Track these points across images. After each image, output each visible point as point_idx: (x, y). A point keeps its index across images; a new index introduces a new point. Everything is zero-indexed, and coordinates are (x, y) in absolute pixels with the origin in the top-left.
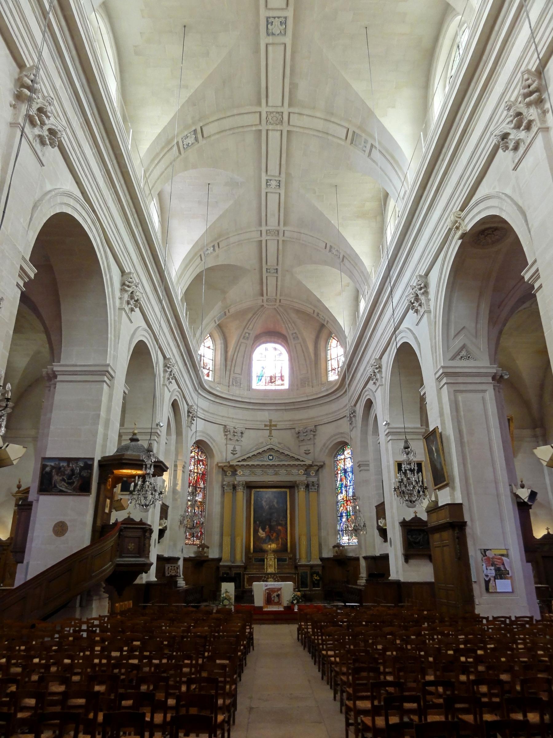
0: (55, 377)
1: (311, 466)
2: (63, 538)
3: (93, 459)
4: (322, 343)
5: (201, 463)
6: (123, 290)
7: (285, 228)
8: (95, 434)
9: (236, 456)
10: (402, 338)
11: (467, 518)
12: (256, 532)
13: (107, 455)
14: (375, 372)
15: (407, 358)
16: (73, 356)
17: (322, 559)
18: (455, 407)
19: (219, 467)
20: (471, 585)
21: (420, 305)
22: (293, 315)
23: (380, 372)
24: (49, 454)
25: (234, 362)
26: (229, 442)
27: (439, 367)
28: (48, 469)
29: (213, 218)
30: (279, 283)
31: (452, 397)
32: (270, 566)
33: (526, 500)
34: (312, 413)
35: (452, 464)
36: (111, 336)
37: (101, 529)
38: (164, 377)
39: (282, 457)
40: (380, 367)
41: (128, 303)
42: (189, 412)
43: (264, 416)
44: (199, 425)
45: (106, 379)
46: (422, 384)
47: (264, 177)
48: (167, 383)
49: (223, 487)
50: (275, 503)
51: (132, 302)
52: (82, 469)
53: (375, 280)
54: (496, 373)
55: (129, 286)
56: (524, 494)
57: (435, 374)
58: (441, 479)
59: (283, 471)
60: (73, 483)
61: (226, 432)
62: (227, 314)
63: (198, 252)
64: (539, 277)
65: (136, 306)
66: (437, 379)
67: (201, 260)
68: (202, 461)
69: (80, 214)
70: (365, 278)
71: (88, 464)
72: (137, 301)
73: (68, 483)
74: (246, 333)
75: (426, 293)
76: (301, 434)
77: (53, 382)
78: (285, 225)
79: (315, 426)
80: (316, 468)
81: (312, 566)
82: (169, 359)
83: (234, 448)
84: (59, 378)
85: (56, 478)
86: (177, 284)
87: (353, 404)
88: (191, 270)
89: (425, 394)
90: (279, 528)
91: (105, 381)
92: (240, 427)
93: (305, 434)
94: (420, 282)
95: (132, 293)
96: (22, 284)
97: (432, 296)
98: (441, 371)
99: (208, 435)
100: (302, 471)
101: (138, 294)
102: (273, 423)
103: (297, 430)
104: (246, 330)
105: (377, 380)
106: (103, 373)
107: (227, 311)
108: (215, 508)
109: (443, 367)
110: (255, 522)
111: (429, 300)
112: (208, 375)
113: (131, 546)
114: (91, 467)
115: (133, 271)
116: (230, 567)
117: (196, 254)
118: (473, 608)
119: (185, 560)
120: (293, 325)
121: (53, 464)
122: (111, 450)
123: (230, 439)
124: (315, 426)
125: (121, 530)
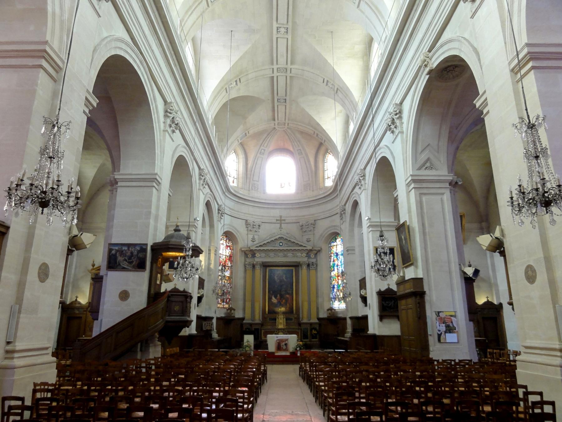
0: (117, 183)
1: (311, 250)
2: (126, 302)
3: (146, 245)
4: (320, 157)
5: (229, 248)
6: (166, 116)
7: (292, 67)
8: (148, 226)
9: (255, 243)
10: (381, 153)
11: (426, 289)
12: (270, 299)
13: (157, 241)
15: (385, 168)
16: (130, 167)
17: (319, 319)
18: (420, 205)
19: (242, 251)
20: (427, 337)
21: (396, 127)
22: (299, 136)
23: (364, 179)
24: (114, 241)
25: (253, 172)
26: (249, 232)
27: (409, 175)
28: (113, 252)
29: (235, 59)
30: (287, 111)
31: (418, 199)
32: (281, 323)
33: (471, 276)
35: (415, 249)
36: (158, 151)
37: (154, 296)
38: (199, 183)
39: (289, 244)
40: (364, 176)
41: (170, 126)
42: (219, 210)
43: (276, 213)
44: (227, 219)
45: (155, 184)
46: (396, 188)
47: (275, 25)
48: (202, 188)
49: (245, 267)
50: (284, 278)
51: (173, 125)
52: (139, 252)
53: (362, 107)
54: (452, 180)
55: (170, 113)
56: (470, 271)
57: (406, 180)
58: (408, 260)
59: (290, 254)
60: (132, 262)
62: (247, 134)
63: (224, 86)
64: (487, 105)
65: (176, 129)
67: (227, 92)
68: (229, 246)
69: (131, 56)
70: (354, 106)
71: (142, 248)
72: (177, 124)
73: (129, 263)
75: (400, 118)
77: (115, 187)
78: (292, 63)
80: (315, 252)
81: (311, 324)
82: (203, 170)
83: (254, 237)
84: (120, 184)
85: (120, 258)
87: (343, 204)
88: (219, 100)
89: (397, 196)
90: (287, 296)
91: (154, 186)
92: (258, 221)
94: (395, 109)
95: (173, 118)
96: (87, 111)
97: (405, 119)
99: (233, 227)
100: (304, 254)
101: (177, 119)
102: (283, 218)
103: (301, 223)
104: (262, 148)
105: (362, 185)
106: (152, 180)
107: (247, 132)
108: (239, 281)
109: (411, 175)
110: (269, 292)
111: (403, 123)
112: (233, 182)
113: (177, 308)
114: (145, 250)
115: (173, 101)
116: (251, 325)
117: (222, 88)
118: (429, 354)
119: (218, 319)
121: (117, 248)
122: (160, 238)
123: (251, 231)
125: (169, 297)
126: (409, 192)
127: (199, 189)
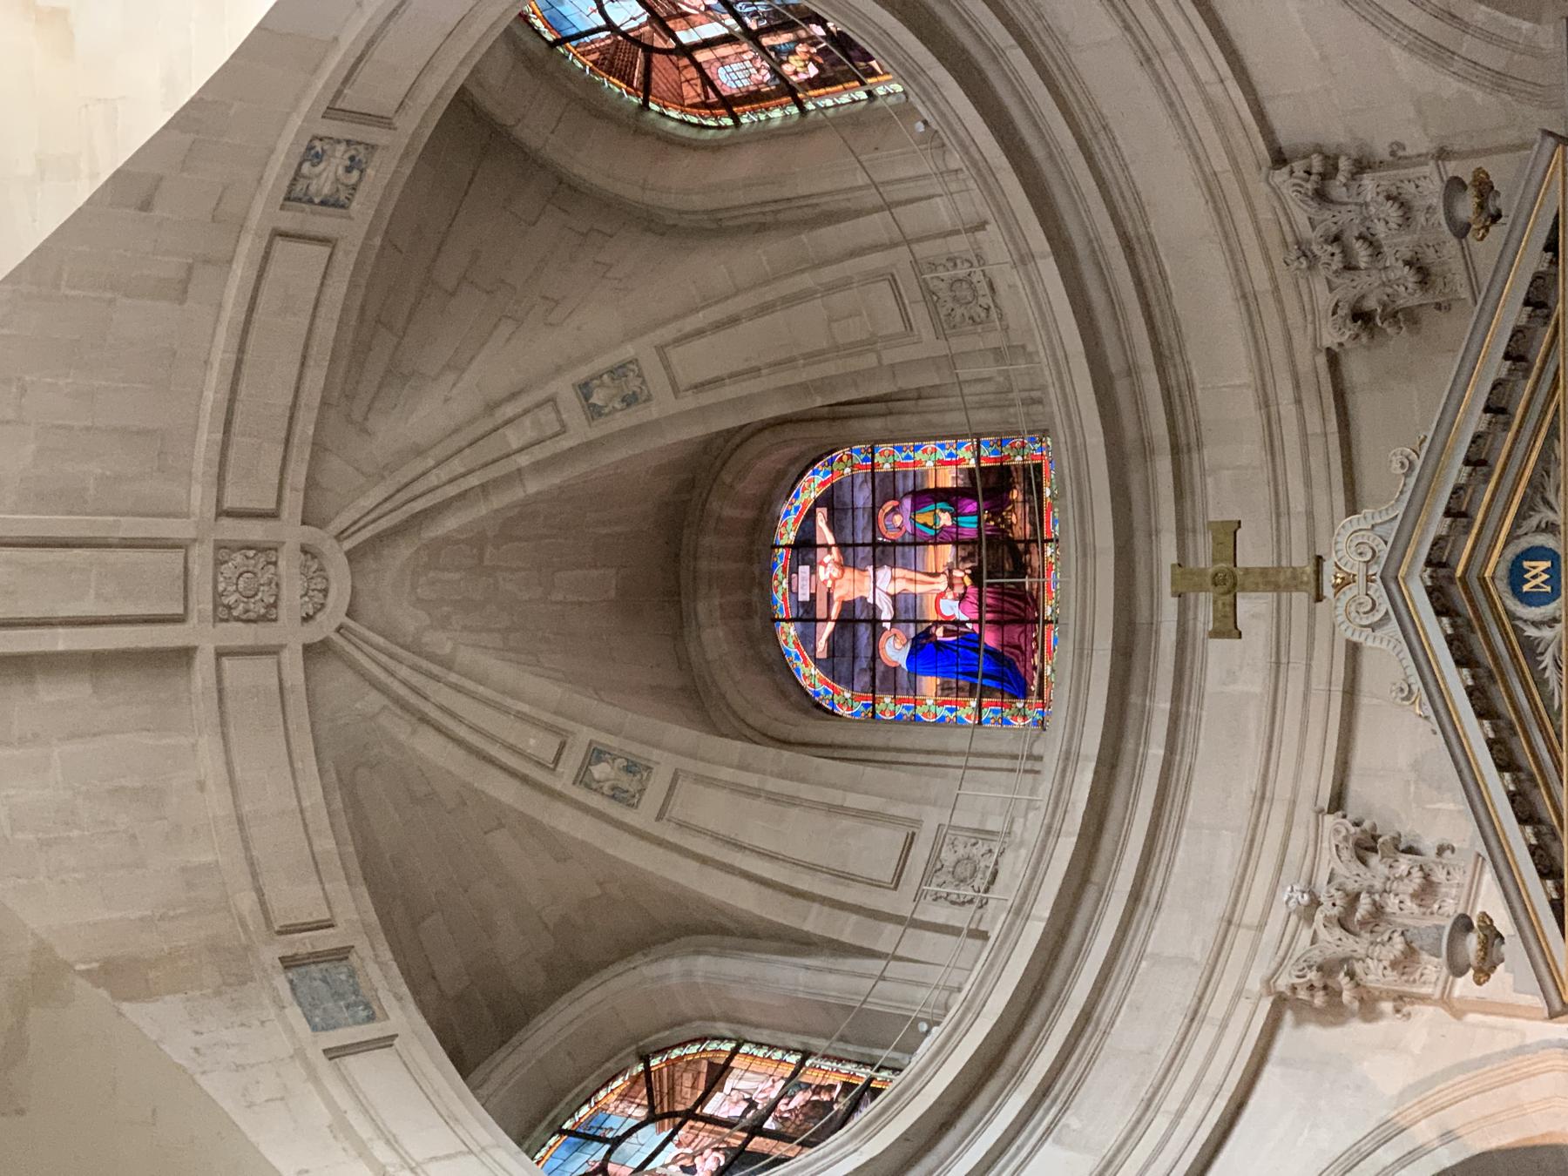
25: (804, 882)
34: (1176, 209)
61: (1333, 993)
74: (583, 778)
76: (1370, 288)
79: (1280, 159)
93: (1362, 254)
104: (563, 781)
120: (509, 410)
124: (1280, 159)
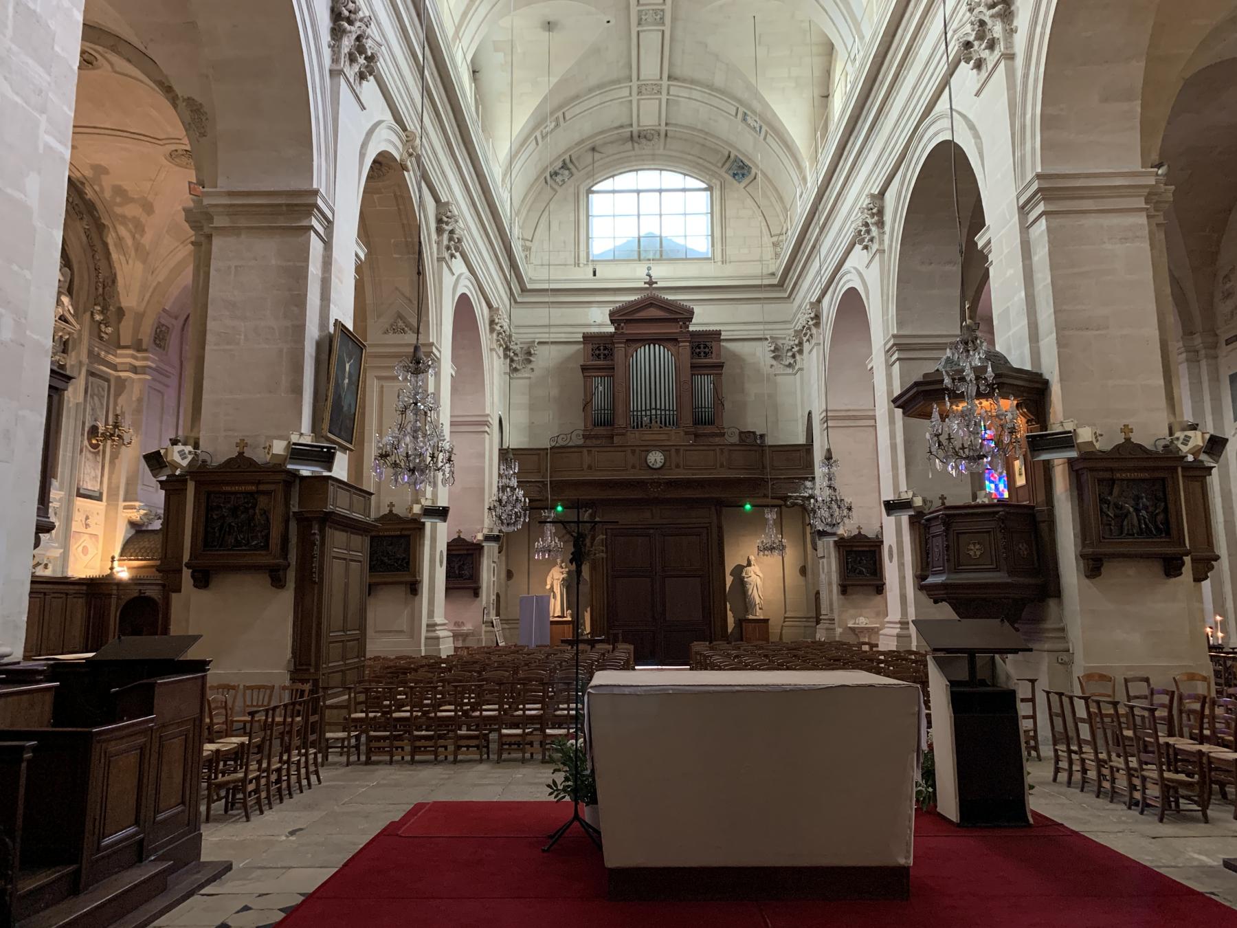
0: (210, 219)
14: (867, 225)
27: (1029, 179)
38: (438, 243)
41: (352, 59)
42: (492, 322)
48: (446, 255)
55: (351, 23)
66: (1023, 207)
84: (219, 221)
86: (454, 40)
89: (989, 242)
95: (358, 38)
98: (1035, 186)
105: (872, 240)
109: (1038, 176)
126: (1025, 228)
127: (440, 259)
